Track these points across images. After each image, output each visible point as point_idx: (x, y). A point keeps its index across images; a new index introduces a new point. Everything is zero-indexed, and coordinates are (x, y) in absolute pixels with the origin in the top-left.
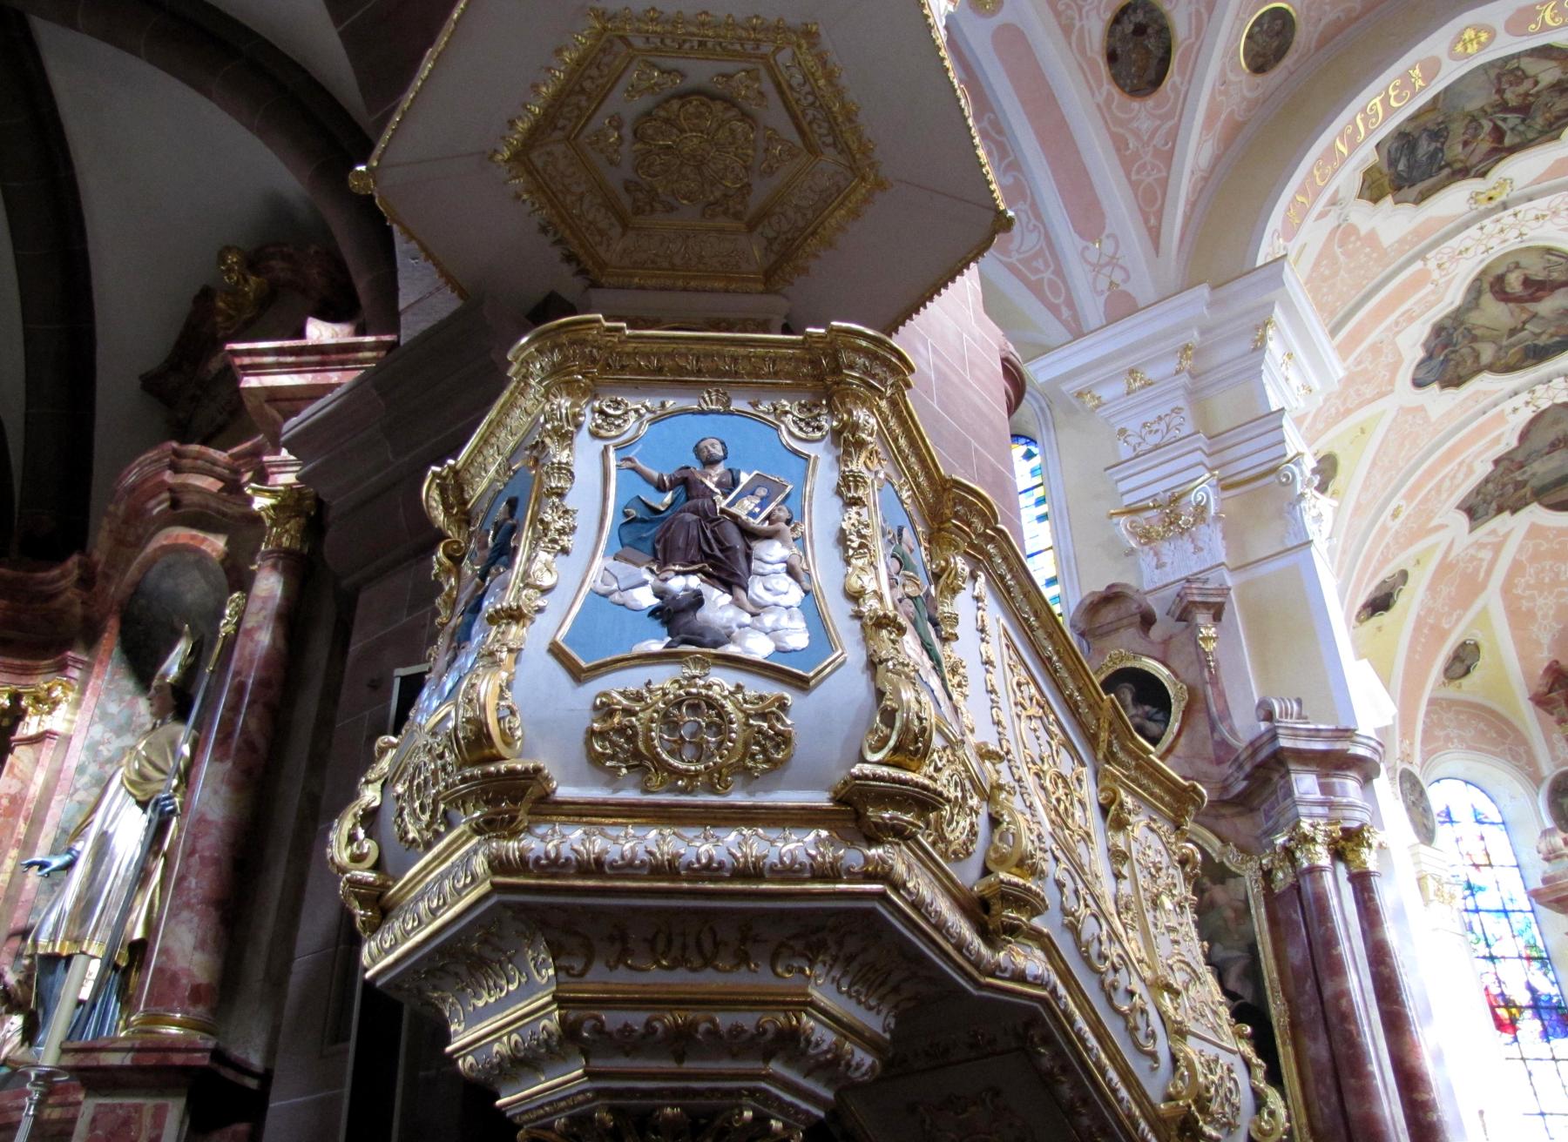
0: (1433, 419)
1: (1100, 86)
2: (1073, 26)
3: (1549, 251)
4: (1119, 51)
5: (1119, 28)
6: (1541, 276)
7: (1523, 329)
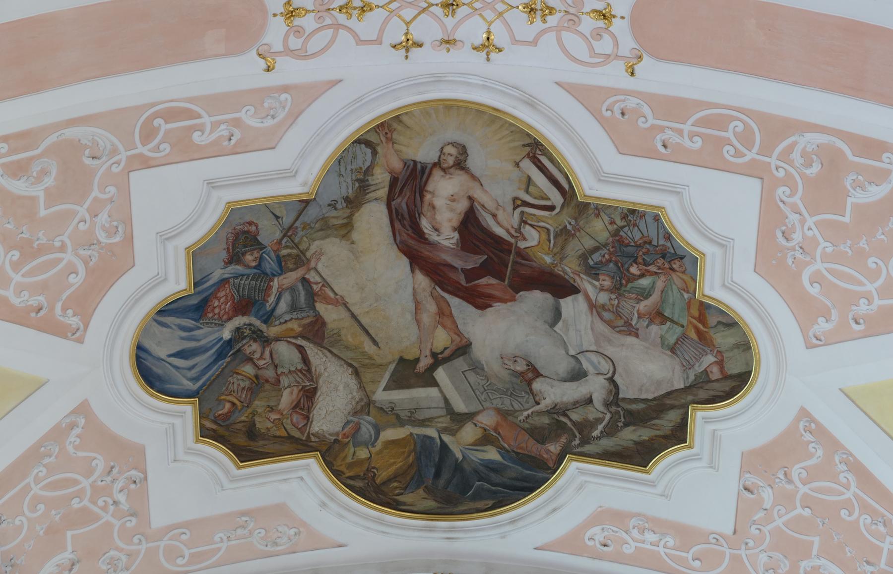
0: (158, 519)
3: (535, 150)
6: (501, 225)
7: (427, 379)
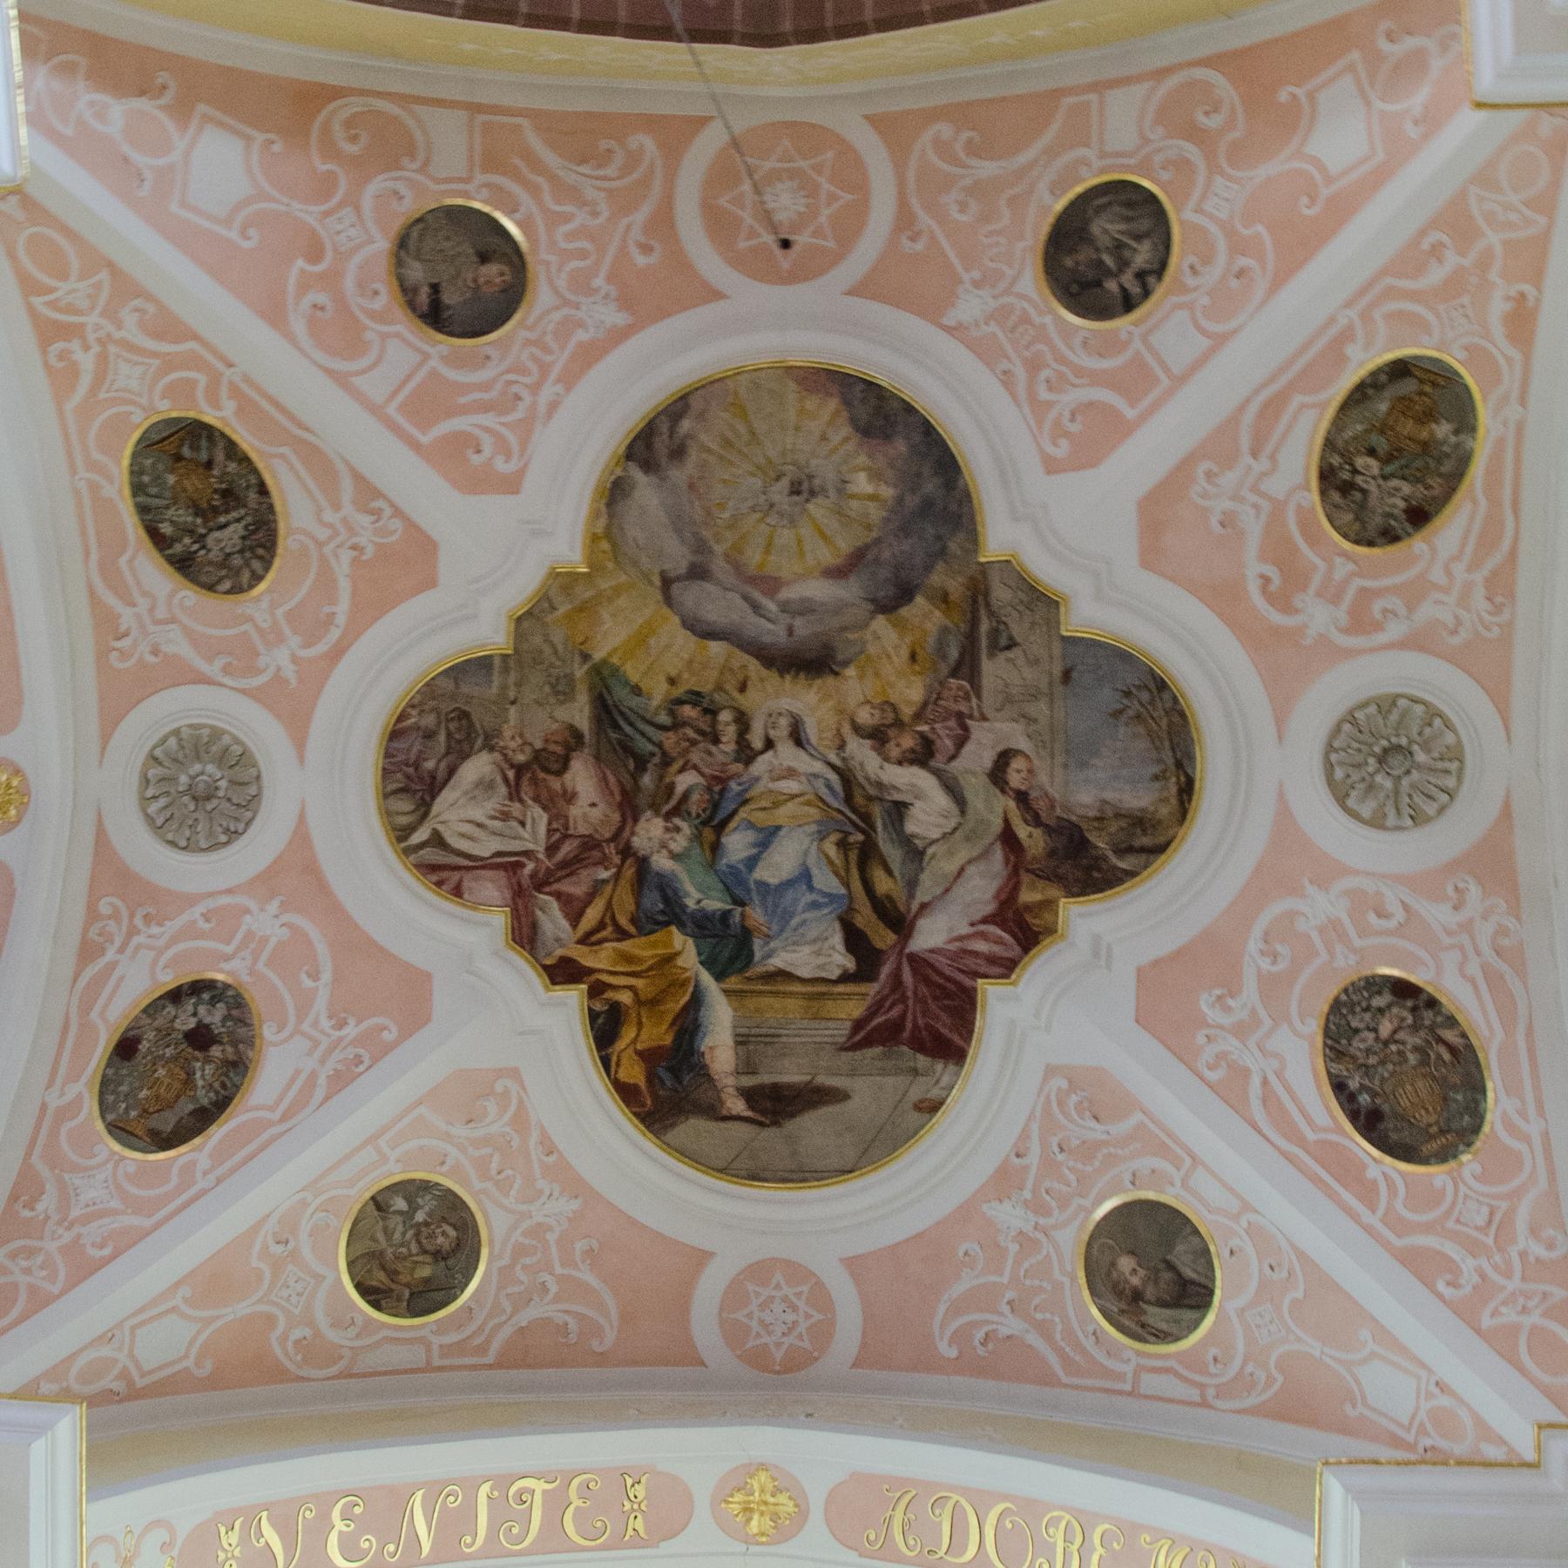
1: (73, 1077)
2: (102, 951)
4: (144, 1046)
5: (170, 1009)
